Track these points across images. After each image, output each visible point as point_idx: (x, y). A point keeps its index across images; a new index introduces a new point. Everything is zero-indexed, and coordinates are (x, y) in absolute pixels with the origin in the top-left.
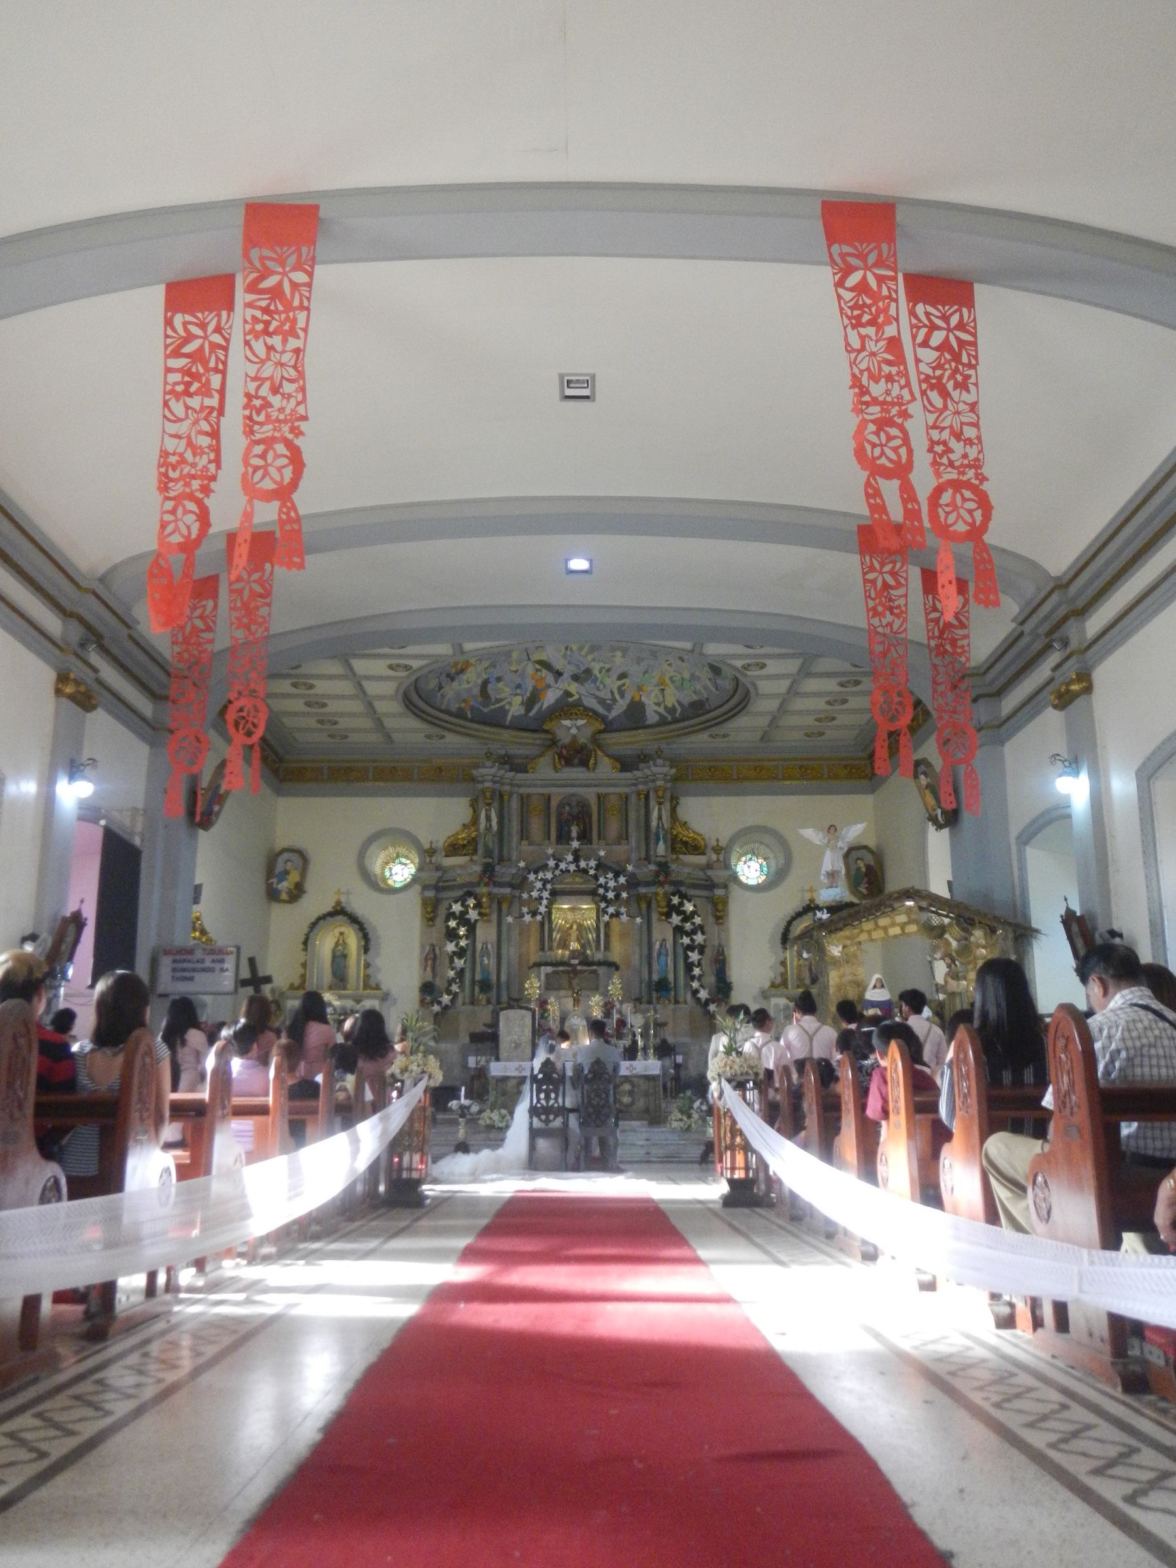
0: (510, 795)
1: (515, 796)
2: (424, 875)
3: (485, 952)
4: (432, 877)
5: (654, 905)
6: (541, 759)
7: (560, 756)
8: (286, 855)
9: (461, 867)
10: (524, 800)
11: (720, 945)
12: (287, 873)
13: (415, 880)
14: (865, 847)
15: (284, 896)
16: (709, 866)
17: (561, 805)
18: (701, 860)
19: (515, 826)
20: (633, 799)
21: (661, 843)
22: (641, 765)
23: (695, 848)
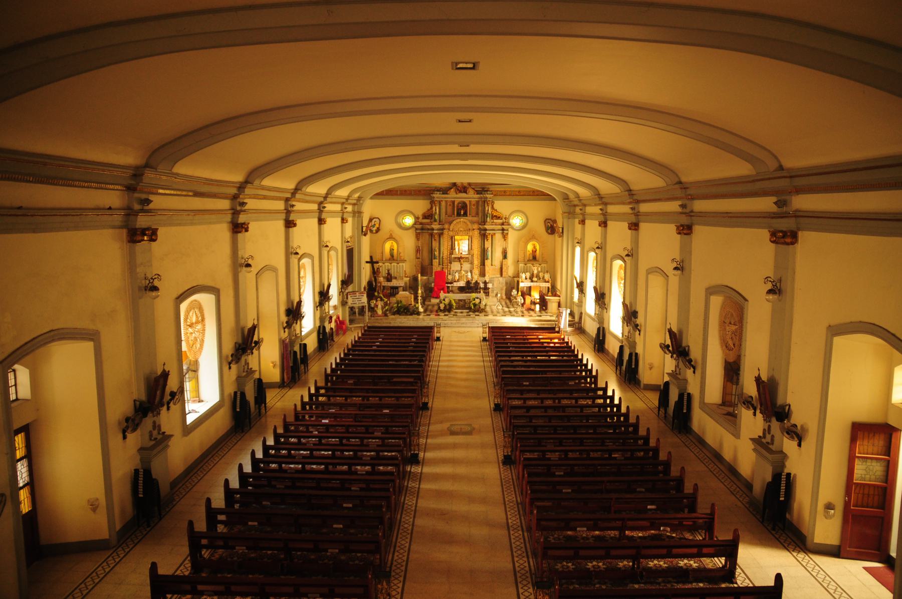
0: (442, 201)
1: (444, 202)
2: (416, 226)
3: (435, 250)
4: (419, 226)
5: (486, 237)
6: (452, 190)
7: (458, 189)
8: (374, 220)
9: (428, 224)
10: (446, 202)
11: (506, 248)
12: (375, 225)
13: (413, 226)
14: (550, 219)
15: (374, 232)
16: (503, 224)
17: (459, 203)
18: (500, 221)
19: (443, 210)
20: (480, 203)
21: (488, 218)
22: (483, 193)
23: (499, 218)
